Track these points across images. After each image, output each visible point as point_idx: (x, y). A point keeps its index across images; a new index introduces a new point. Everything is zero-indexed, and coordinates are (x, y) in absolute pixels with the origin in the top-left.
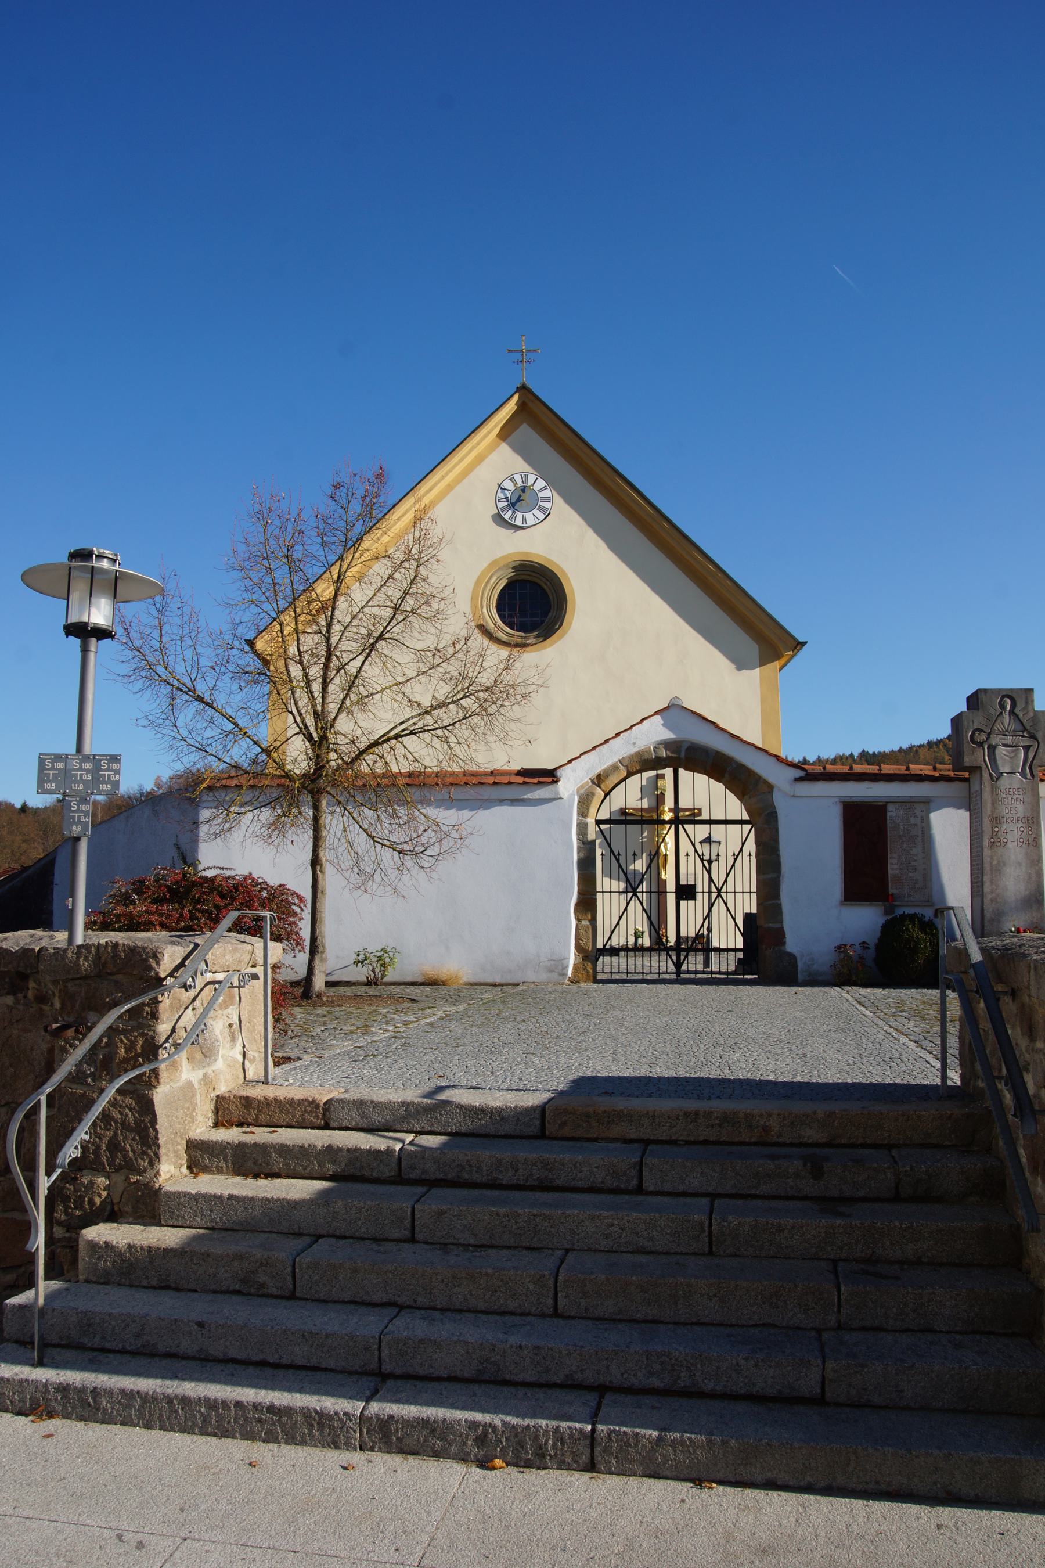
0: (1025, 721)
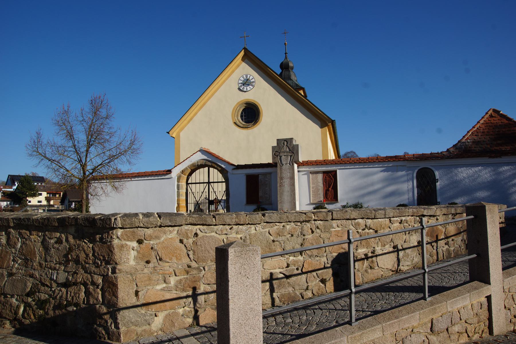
0: (290, 148)
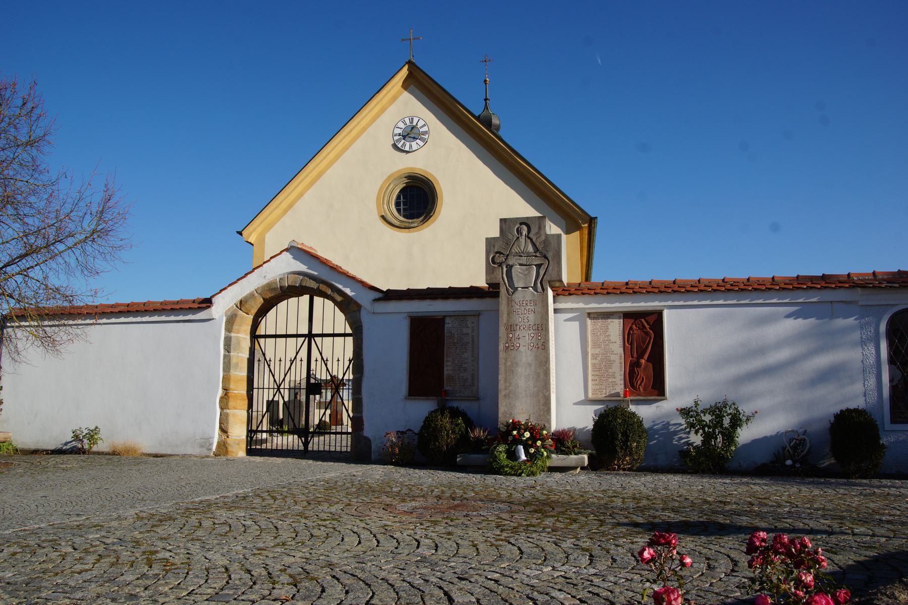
0: (538, 244)
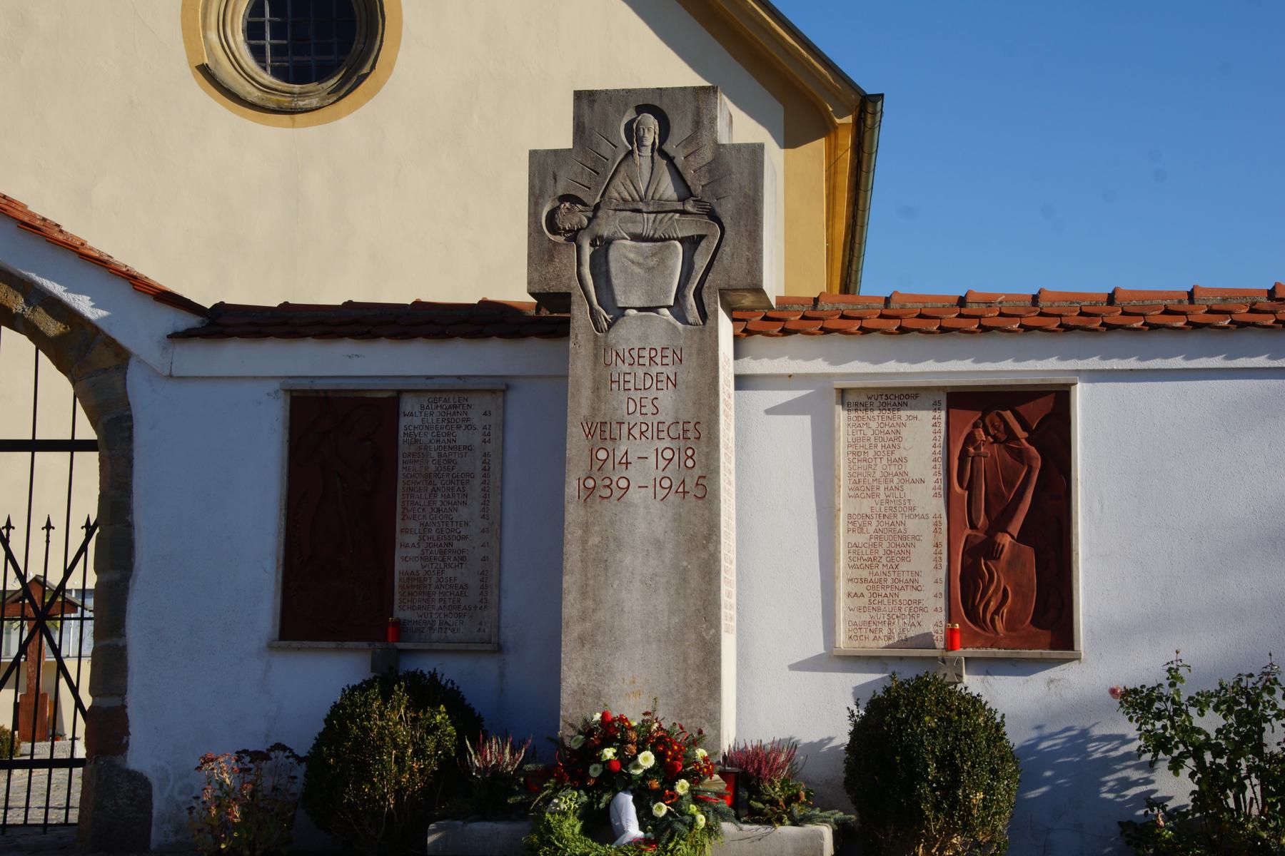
0: (689, 175)
